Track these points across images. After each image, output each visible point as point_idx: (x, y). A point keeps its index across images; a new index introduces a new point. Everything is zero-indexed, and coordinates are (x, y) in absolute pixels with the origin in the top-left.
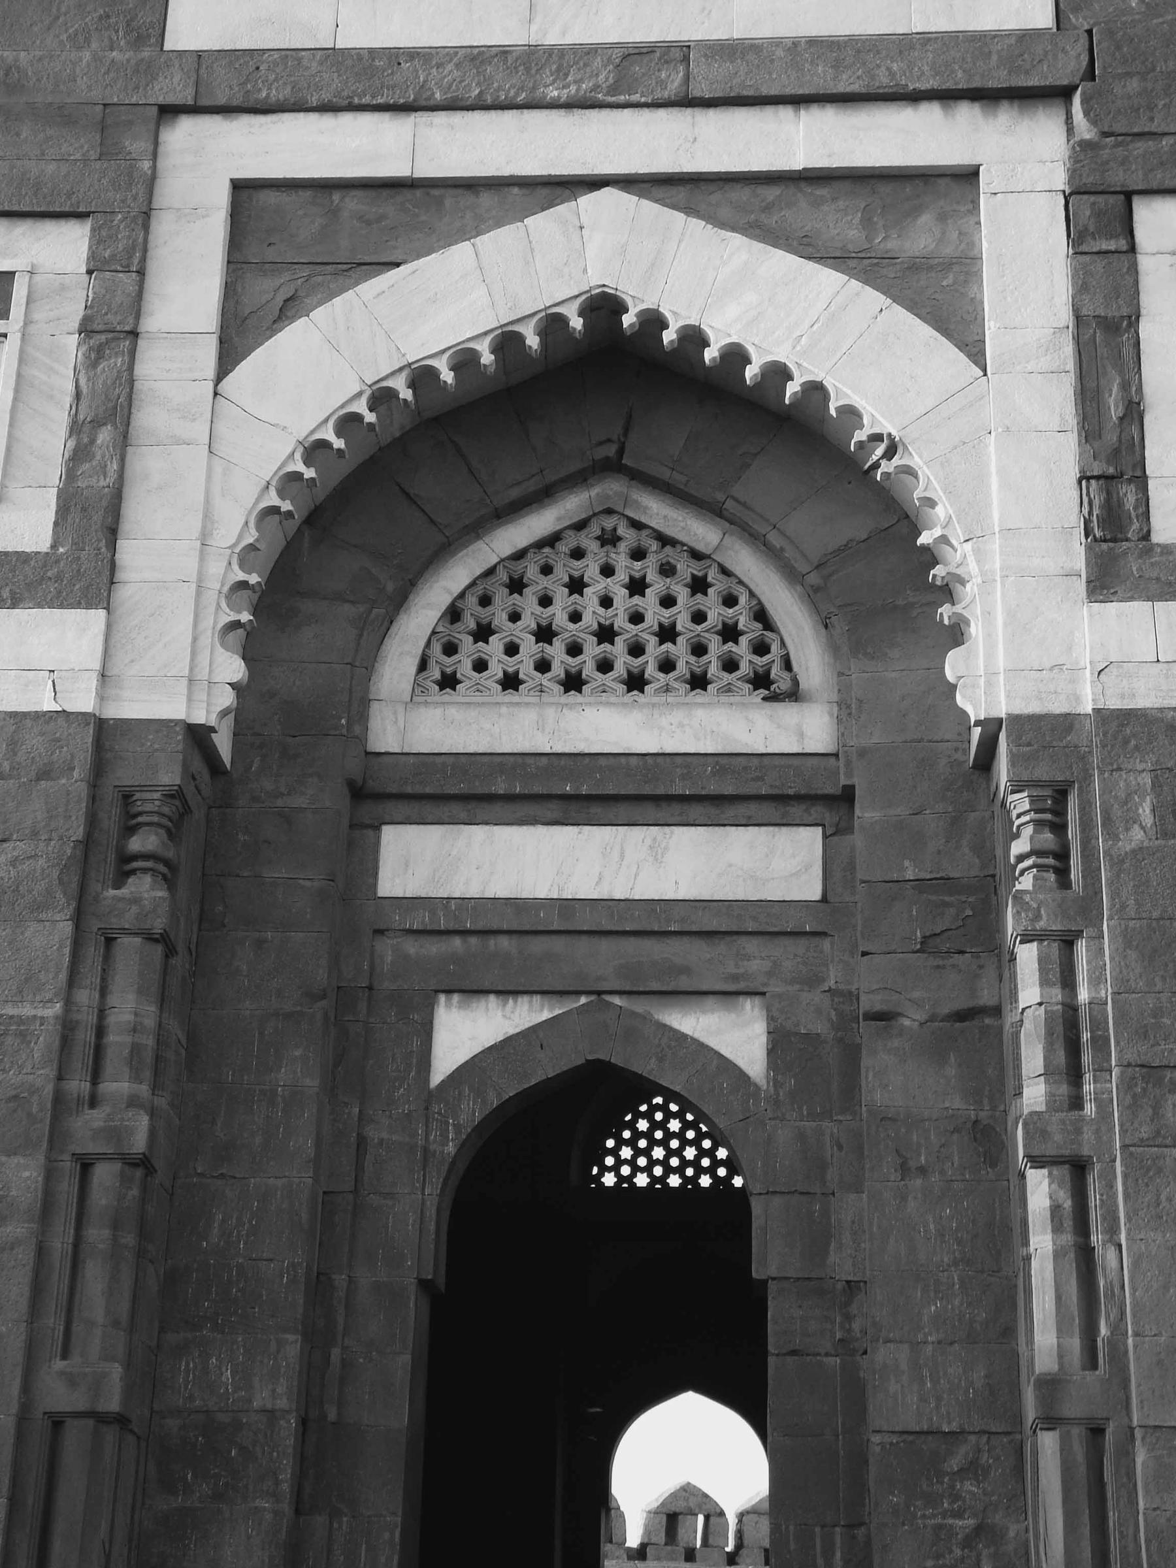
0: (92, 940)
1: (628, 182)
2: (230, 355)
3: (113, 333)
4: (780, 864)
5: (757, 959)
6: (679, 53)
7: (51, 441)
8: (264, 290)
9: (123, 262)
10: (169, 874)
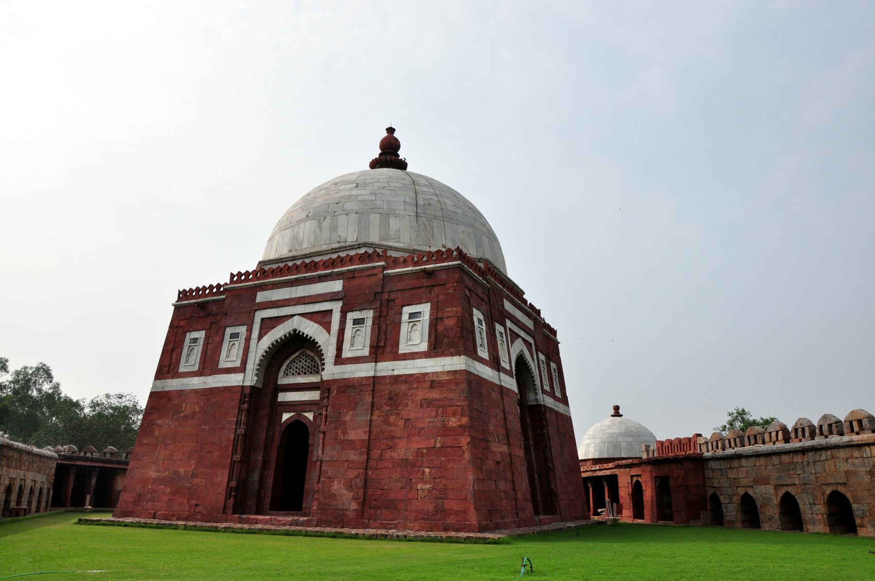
0: (240, 411)
1: (299, 315)
3: (248, 339)
4: (315, 395)
5: (313, 407)
6: (304, 297)
7: (241, 353)
8: (264, 331)
9: (250, 330)
10: (250, 403)
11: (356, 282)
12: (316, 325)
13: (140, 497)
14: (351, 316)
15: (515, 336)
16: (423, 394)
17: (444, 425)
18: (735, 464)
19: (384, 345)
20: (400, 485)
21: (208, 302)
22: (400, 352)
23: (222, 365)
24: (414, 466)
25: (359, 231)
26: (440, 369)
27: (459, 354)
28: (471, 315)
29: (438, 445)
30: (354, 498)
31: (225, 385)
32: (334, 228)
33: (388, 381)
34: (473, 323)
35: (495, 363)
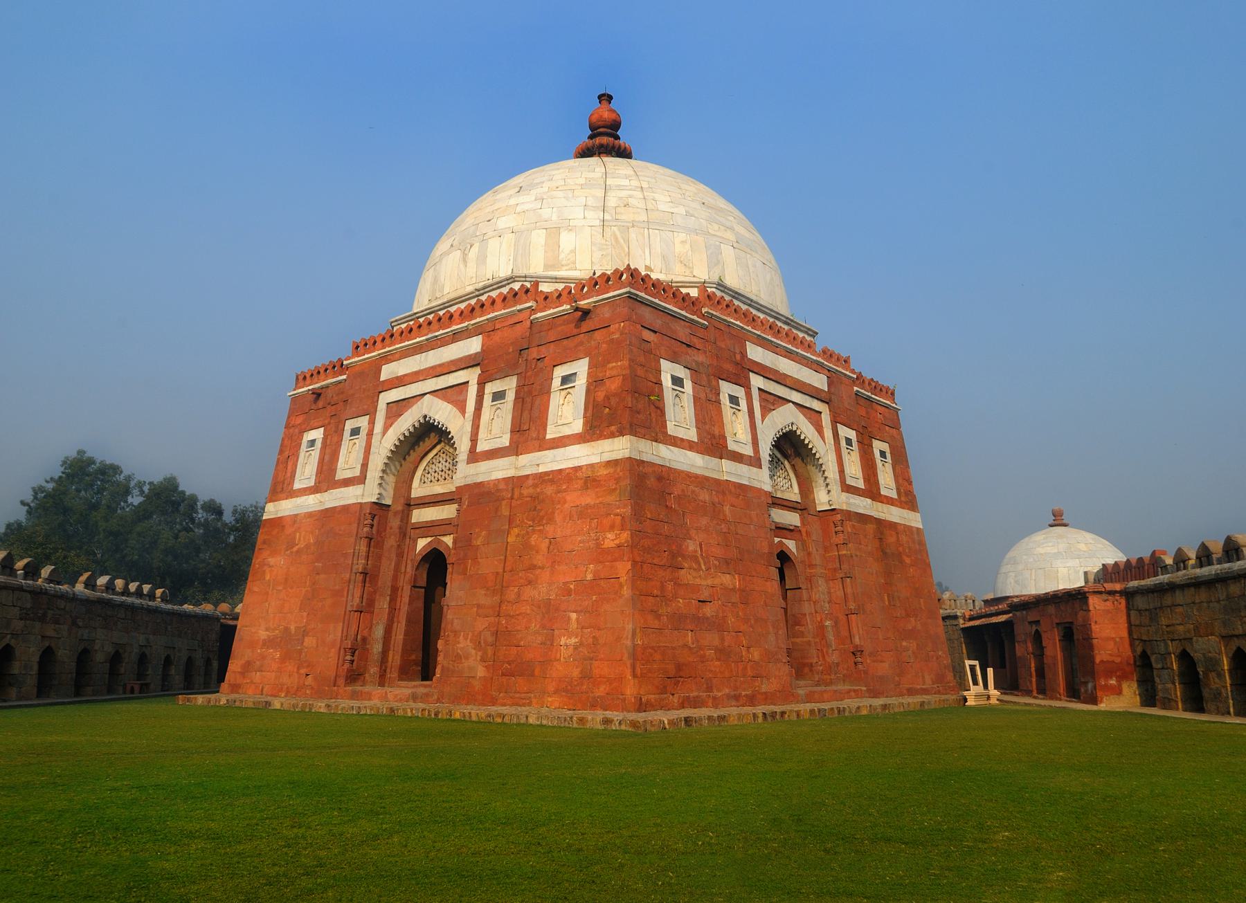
2: (384, 433)
3: (370, 434)
5: (450, 528)
6: (433, 368)
9: (372, 422)
10: (372, 526)
11: (497, 337)
12: (450, 406)
13: (248, 667)
14: (491, 388)
15: (771, 402)
16: (575, 498)
17: (598, 545)
18: (1168, 600)
19: (528, 430)
20: (540, 639)
21: (327, 387)
22: (548, 437)
23: (341, 475)
24: (557, 610)
25: (515, 260)
26: (595, 459)
27: (622, 434)
28: (658, 371)
29: (589, 577)
30: (483, 660)
31: (342, 503)
32: (482, 259)
33: (530, 482)
34: (659, 383)
35: (713, 444)
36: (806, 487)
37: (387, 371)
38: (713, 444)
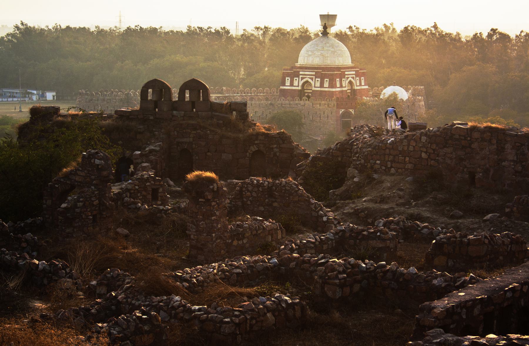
14: (317, 79)
15: (348, 78)
19: (322, 86)
36: (352, 87)
37: (301, 73)
38: (341, 86)
